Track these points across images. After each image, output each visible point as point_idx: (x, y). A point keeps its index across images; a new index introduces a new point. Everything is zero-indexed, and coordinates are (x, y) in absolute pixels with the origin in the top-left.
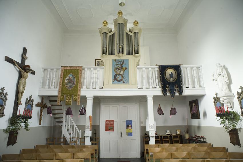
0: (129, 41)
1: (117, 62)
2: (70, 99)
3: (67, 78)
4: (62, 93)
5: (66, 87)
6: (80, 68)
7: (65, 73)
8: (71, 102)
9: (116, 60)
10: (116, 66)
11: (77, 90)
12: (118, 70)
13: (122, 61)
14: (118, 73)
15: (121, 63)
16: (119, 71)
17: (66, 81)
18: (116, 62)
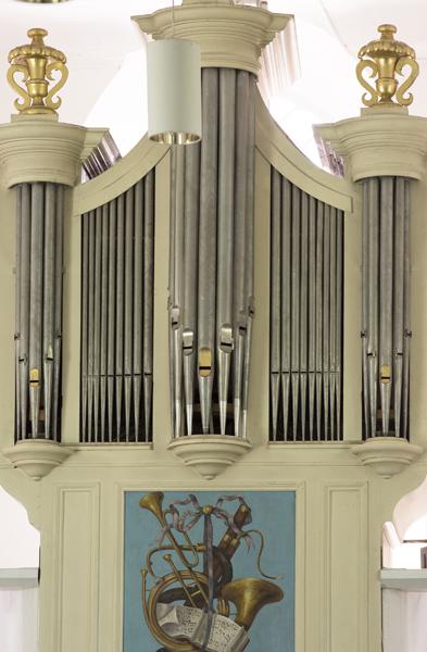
0: (305, 277)
1: (169, 518)
9: (159, 496)
10: (162, 568)
12: (181, 603)
13: (231, 508)
14: (183, 640)
15: (219, 533)
16: (197, 616)
18: (161, 515)
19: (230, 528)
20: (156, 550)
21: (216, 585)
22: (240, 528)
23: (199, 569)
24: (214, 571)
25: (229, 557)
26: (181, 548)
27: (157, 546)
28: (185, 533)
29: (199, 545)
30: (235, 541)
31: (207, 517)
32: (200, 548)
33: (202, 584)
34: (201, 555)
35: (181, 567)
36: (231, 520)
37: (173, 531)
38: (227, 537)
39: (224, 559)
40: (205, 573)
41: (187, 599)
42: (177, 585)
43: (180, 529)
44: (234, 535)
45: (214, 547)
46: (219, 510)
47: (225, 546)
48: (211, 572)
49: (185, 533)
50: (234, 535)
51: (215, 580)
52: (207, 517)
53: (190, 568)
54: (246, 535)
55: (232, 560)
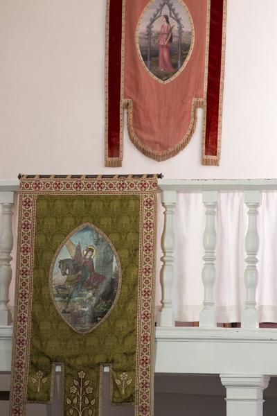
2: (89, 390)
3: (65, 254)
4: (38, 352)
5: (60, 312)
6: (143, 186)
7: (50, 222)
8: (96, 407)
11: (132, 332)
17: (58, 276)
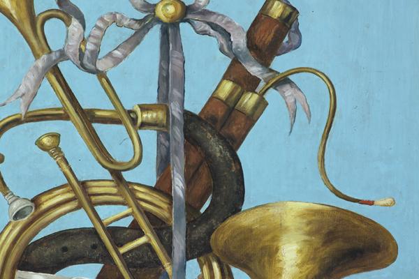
1: (54, 30)
19: (236, 62)
20: (17, 122)
21: (194, 219)
22: (265, 61)
23: (146, 174)
24: (189, 181)
25: (233, 143)
26: (88, 118)
27: (19, 109)
28: (101, 75)
29: (144, 108)
30: (250, 100)
31: (169, 33)
32: (148, 116)
33: (152, 218)
34: (150, 137)
35: (89, 168)
36: (240, 41)
37: (66, 68)
38: (228, 86)
39: (217, 149)
40: (163, 188)
41: (105, 258)
42: (79, 220)
43: (87, 63)
44: (249, 83)
45: (188, 115)
46: (206, 13)
47: (220, 113)
48: (179, 185)
49: (101, 75)
50: (249, 83)
51: (191, 207)
52: (169, 33)
53: (117, 175)
54: (283, 81)
55: (240, 153)
